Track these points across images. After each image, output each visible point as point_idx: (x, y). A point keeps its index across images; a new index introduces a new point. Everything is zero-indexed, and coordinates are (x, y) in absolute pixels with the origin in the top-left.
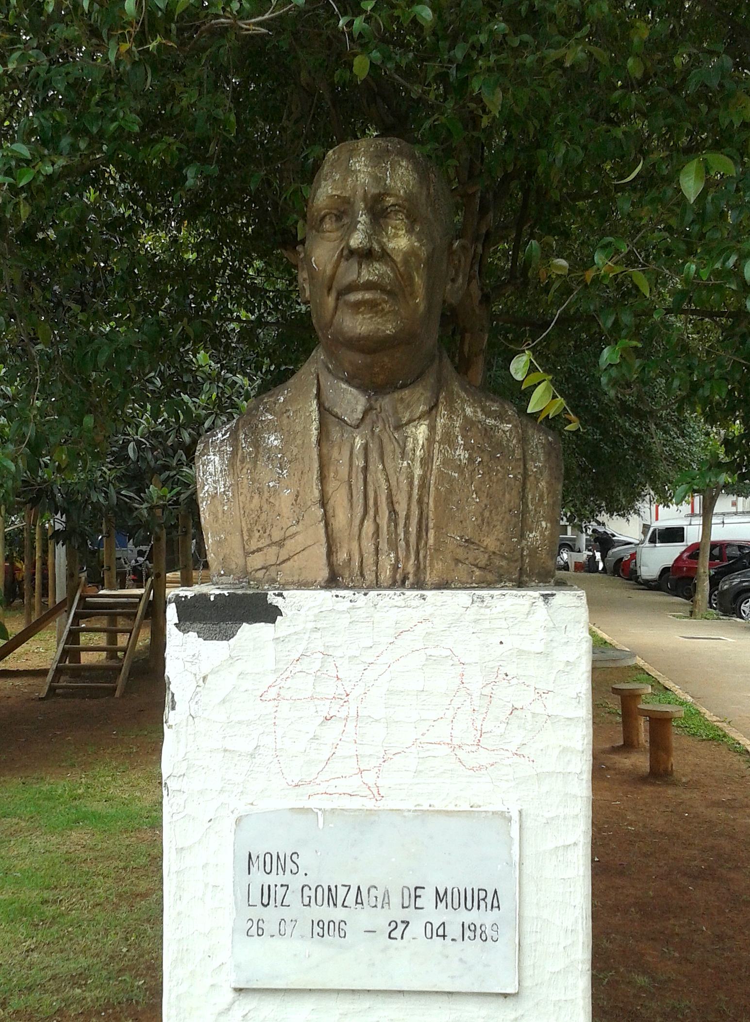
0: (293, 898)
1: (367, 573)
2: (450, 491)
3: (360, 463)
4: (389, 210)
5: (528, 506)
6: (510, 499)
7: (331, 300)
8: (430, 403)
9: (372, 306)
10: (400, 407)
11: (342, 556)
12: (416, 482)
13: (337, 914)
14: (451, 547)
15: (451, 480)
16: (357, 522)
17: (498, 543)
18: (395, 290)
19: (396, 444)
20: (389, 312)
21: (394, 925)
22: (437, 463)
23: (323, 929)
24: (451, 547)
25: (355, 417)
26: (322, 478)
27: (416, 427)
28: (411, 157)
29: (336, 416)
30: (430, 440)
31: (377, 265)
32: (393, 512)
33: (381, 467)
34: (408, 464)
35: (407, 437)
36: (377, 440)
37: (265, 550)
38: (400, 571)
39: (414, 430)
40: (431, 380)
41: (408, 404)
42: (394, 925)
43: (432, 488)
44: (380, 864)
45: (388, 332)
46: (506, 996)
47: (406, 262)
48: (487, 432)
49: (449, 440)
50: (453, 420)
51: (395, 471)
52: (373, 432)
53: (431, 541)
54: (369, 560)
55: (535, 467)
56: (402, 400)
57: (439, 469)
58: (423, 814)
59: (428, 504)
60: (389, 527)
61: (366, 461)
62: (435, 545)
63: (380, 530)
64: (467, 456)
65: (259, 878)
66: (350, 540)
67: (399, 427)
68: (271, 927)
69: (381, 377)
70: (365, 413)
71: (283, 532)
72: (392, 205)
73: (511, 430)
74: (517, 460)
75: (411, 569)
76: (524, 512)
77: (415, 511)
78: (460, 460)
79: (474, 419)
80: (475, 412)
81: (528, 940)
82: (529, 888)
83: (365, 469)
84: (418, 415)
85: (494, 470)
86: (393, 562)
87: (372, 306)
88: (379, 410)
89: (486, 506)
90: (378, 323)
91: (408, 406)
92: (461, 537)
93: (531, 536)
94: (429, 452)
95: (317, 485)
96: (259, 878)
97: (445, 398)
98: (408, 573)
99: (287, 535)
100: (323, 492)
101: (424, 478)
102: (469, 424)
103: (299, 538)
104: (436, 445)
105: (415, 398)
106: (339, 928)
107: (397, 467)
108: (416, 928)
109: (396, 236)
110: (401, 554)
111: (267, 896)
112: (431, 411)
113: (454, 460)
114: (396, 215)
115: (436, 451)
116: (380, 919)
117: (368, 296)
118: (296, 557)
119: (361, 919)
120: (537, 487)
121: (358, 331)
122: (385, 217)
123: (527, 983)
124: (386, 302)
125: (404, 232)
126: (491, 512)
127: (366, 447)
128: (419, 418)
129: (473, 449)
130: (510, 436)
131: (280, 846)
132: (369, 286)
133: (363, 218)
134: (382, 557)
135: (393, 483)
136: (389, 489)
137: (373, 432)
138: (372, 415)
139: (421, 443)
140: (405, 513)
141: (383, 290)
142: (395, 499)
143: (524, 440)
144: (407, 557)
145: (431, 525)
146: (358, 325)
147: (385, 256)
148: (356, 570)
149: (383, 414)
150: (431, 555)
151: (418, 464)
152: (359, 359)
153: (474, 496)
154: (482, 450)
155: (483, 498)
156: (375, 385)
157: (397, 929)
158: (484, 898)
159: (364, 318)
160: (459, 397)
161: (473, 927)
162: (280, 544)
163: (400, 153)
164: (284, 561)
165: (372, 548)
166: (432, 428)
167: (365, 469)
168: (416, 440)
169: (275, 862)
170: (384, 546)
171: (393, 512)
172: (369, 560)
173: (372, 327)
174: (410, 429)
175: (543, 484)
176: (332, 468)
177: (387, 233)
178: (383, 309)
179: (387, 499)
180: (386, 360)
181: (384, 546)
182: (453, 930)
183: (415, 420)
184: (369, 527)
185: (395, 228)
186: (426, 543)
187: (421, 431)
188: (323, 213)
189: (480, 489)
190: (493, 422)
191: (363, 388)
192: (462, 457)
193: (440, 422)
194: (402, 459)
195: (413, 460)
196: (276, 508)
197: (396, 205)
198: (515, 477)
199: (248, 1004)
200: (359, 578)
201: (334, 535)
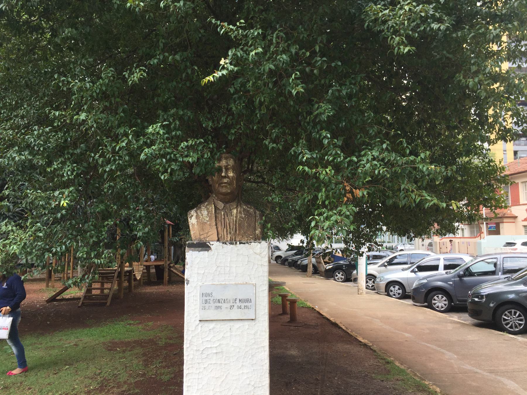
0: (211, 302)
3: (223, 217)
6: (253, 224)
7: (217, 185)
9: (226, 186)
11: (220, 236)
13: (220, 305)
18: (230, 184)
21: (231, 306)
22: (238, 217)
23: (217, 308)
26: (216, 220)
28: (233, 158)
40: (236, 201)
42: (231, 306)
44: (229, 294)
46: (253, 320)
48: (248, 211)
49: (240, 213)
58: (236, 284)
65: (205, 298)
68: (207, 308)
77: (234, 227)
81: (257, 309)
82: (257, 298)
87: (226, 186)
96: (205, 298)
100: (216, 223)
101: (236, 220)
102: (244, 210)
106: (220, 307)
108: (235, 307)
111: (206, 302)
112: (237, 208)
116: (228, 305)
119: (224, 305)
123: (257, 317)
127: (224, 214)
131: (209, 292)
132: (225, 183)
133: (224, 170)
143: (255, 213)
146: (224, 190)
147: (228, 177)
152: (222, 196)
156: (226, 202)
157: (232, 307)
158: (248, 301)
161: (246, 306)
162: (207, 233)
163: (231, 157)
166: (237, 210)
169: (207, 295)
170: (228, 233)
174: (233, 211)
181: (228, 233)
182: (243, 307)
184: (225, 230)
187: (235, 211)
191: (223, 202)
193: (239, 209)
199: (202, 323)
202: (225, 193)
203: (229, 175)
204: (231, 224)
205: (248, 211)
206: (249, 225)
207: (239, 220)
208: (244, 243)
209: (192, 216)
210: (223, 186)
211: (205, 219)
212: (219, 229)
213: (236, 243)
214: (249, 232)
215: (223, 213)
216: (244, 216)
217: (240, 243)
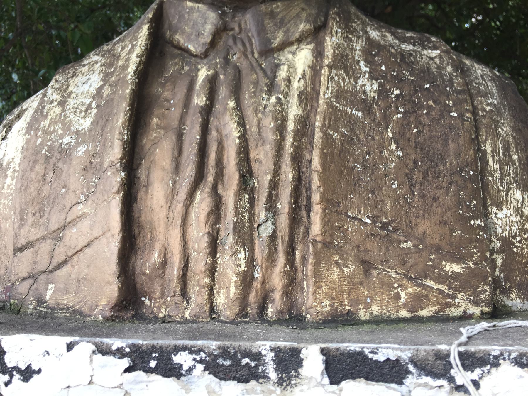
1: (193, 290)
2: (348, 140)
3: (199, 100)
5: (487, 163)
8: (315, 22)
10: (269, 24)
12: (291, 126)
14: (356, 238)
15: (352, 121)
16: (182, 194)
17: (446, 230)
19: (261, 74)
22: (326, 94)
24: (356, 238)
27: (294, 53)
29: (179, 47)
32: (246, 176)
33: (232, 104)
34: (278, 99)
35: (277, 66)
36: (230, 70)
37: (37, 246)
38: (257, 285)
39: (290, 56)
43: (318, 137)
49: (343, 62)
50: (351, 40)
51: (256, 111)
53: (316, 228)
54: (199, 262)
55: (488, 104)
56: (272, 15)
57: (329, 105)
59: (310, 161)
60: (237, 202)
62: (324, 233)
63: (223, 207)
64: (376, 87)
66: (168, 225)
67: (268, 51)
71: (63, 217)
73: (440, 57)
74: (459, 92)
75: (277, 281)
76: (483, 171)
77: (288, 174)
78: (365, 92)
79: (382, 42)
83: (208, 111)
84: (297, 35)
85: (422, 107)
86: (243, 268)
88: (237, 29)
89: (415, 162)
91: (281, 24)
92: (374, 220)
93: (500, 215)
94: (313, 83)
95: (120, 133)
97: (338, 14)
98: (273, 291)
99: (68, 220)
103: (84, 225)
104: (325, 71)
107: (259, 105)
110: (261, 250)
113: (355, 94)
115: (324, 79)
118: (75, 258)
120: (496, 135)
126: (426, 174)
127: (212, 83)
128: (299, 41)
129: (385, 78)
130: (442, 62)
134: (224, 259)
135: (253, 129)
136: (244, 137)
137: (227, 61)
138: (226, 40)
139: (300, 71)
140: (268, 177)
142: (253, 154)
144: (271, 259)
145: (316, 197)
148: (175, 284)
149: (243, 35)
150: (316, 254)
151: (294, 100)
153: (393, 147)
154: (399, 81)
155: (411, 151)
162: (56, 236)
164: (60, 265)
165: (205, 242)
166: (318, 54)
167: (208, 111)
171: (246, 176)
172: (199, 262)
174: (286, 56)
175: (505, 129)
176: (157, 111)
179: (239, 153)
183: (291, 44)
184: (202, 203)
186: (307, 230)
187: (302, 58)
189: (403, 135)
190: (411, 47)
192: (368, 88)
194: (270, 93)
195: (286, 95)
196: (63, 177)
198: (461, 116)
200: (178, 299)
201: (143, 218)
204: (262, 156)
205: (404, 59)
206: (425, 160)
207: (334, 116)
208: (392, 372)
209: (19, 117)
211: (67, 127)
212: (156, 197)
213: (289, 363)
214: (425, 226)
216: (371, 88)
217: (340, 368)
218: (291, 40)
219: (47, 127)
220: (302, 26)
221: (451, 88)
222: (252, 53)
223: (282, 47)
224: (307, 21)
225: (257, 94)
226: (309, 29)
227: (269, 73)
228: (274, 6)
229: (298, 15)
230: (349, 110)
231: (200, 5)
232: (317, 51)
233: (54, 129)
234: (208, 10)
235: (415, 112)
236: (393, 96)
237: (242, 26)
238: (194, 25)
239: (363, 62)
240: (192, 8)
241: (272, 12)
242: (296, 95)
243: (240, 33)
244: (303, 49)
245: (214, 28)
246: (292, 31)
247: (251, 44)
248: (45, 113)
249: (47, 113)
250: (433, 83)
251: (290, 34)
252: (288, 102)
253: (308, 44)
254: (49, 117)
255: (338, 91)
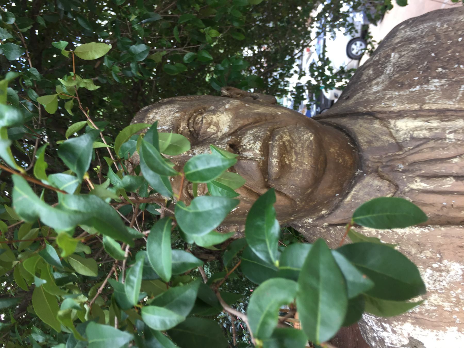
4: (192, 129)
8: (371, 119)
9: (285, 150)
20: (290, 136)
25: (387, 187)
27: (398, 131)
30: (415, 115)
31: (245, 142)
33: (455, 160)
35: (412, 138)
36: (416, 167)
41: (372, 137)
45: (312, 138)
47: (244, 117)
52: (404, 171)
56: (369, 142)
57: (459, 102)
61: (447, 176)
64: (436, 80)
69: (347, 158)
70: (382, 177)
72: (188, 125)
78: (442, 85)
80: (377, 84)
84: (385, 128)
87: (285, 150)
88: (379, 164)
90: (302, 147)
94: (431, 116)
105: (367, 131)
107: (456, 143)
109: (217, 125)
114: (197, 123)
117: (275, 153)
121: (308, 168)
122: (198, 134)
124: (282, 137)
125: (214, 117)
127: (426, 177)
128: (388, 128)
132: (266, 150)
137: (404, 171)
141: (271, 137)
149: (384, 160)
151: (450, 124)
152: (329, 178)
159: (296, 160)
160: (361, 98)
166: (400, 115)
168: (416, 129)
173: (306, 153)
174: (401, 136)
177: (214, 134)
178: (288, 141)
180: (332, 150)
183: (390, 132)
185: (210, 124)
188: (185, 195)
193: (396, 107)
197: (188, 121)
202: (316, 160)
203: (225, 129)
210: (283, 166)
215: (419, 185)
218: (388, 132)
219: (451, 304)
220: (376, 126)
221: (434, 43)
222: (399, 155)
223: (394, 138)
224: (371, 123)
225: (445, 146)
226: (379, 121)
227: (421, 142)
228: (362, 141)
229: (367, 129)
230: (461, 92)
231: (354, 189)
232: (396, 117)
233: (455, 297)
234: (362, 182)
235: (458, 59)
236: (444, 71)
237: (377, 161)
238: (368, 195)
239: (411, 90)
240: (353, 197)
241: (367, 142)
242: (446, 123)
243: (382, 163)
244: (395, 126)
245: (378, 178)
246: (381, 131)
247: (393, 156)
248: (435, 308)
249: (435, 306)
250: (430, 52)
251: (384, 132)
252: (450, 128)
253: (390, 123)
254: (441, 303)
255: (445, 99)
